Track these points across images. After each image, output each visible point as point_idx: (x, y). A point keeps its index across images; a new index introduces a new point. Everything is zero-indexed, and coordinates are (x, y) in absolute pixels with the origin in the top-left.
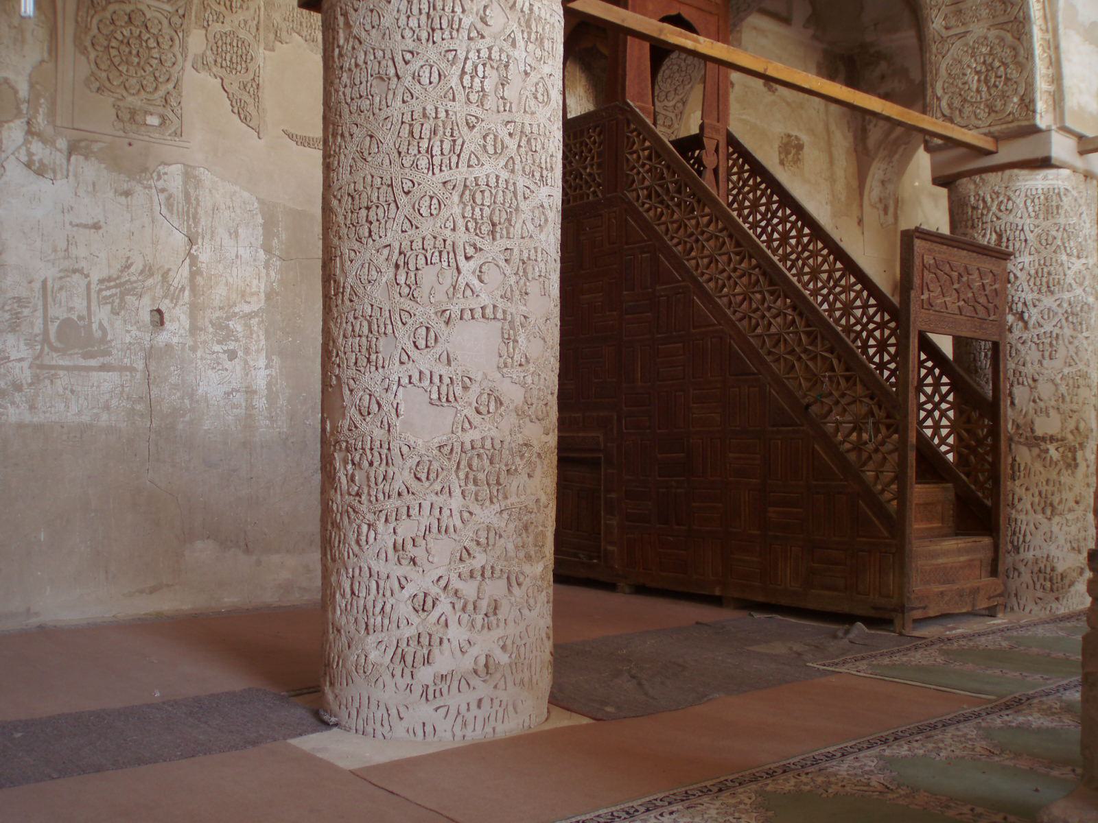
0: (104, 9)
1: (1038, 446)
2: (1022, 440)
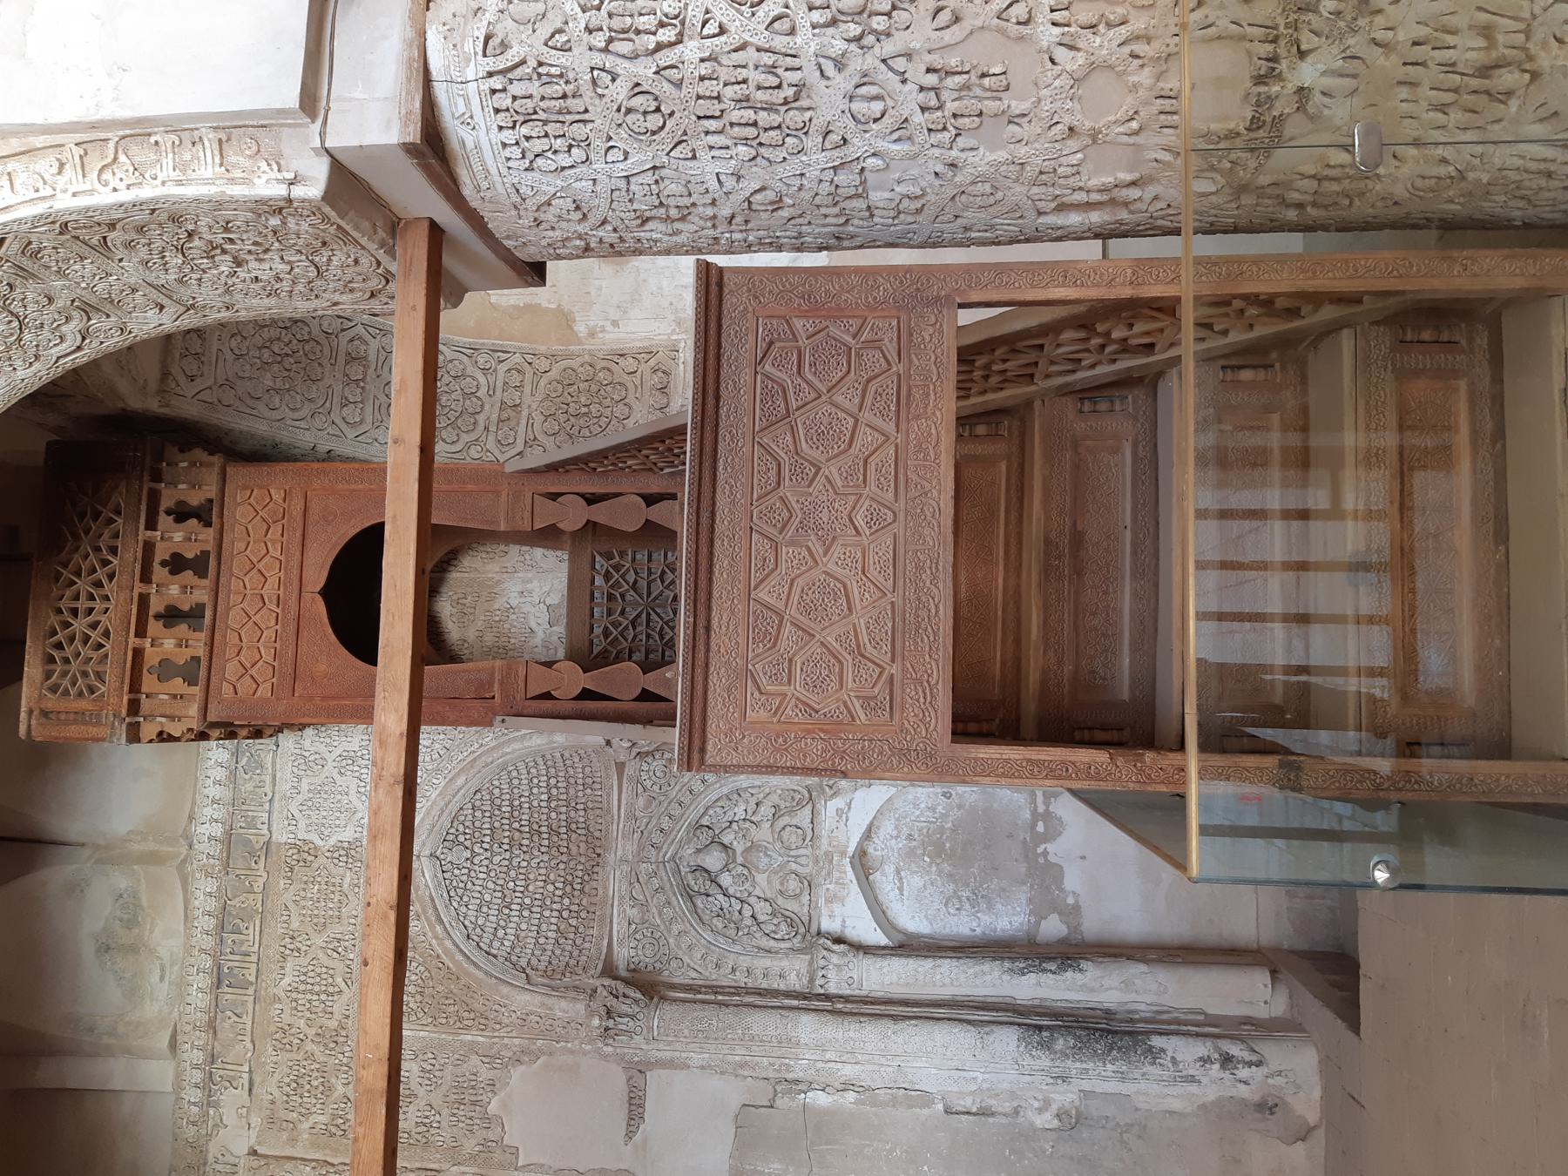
1: (1279, 121)
2: (1252, 164)
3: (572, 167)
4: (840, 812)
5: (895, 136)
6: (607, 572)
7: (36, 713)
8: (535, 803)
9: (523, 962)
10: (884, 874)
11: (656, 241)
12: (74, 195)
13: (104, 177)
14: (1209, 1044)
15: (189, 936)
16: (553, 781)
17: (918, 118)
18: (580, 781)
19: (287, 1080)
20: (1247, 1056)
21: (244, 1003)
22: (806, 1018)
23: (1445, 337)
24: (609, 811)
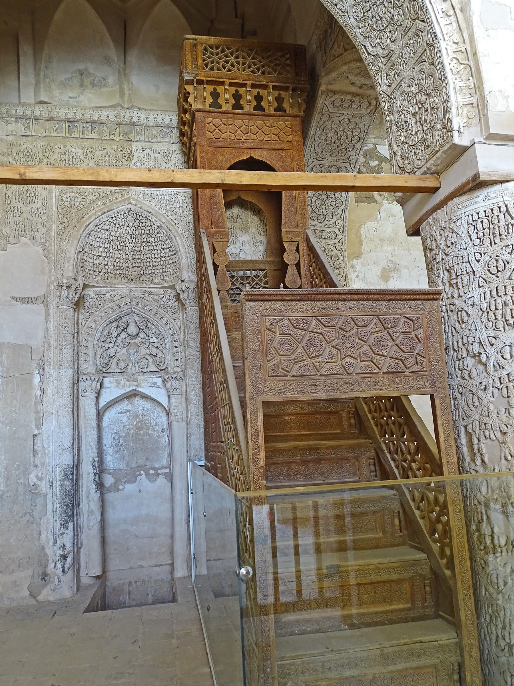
3: (471, 240)
4: (155, 383)
5: (496, 364)
6: (259, 276)
7: (195, 42)
8: (153, 252)
9: (86, 250)
10: (127, 405)
11: (438, 276)
12: (446, 48)
13: (454, 60)
14: (71, 549)
16: (163, 259)
17: (505, 373)
19: (30, 151)
20: (67, 566)
21: (62, 132)
22: (71, 371)
23: (428, 596)
24: (151, 283)
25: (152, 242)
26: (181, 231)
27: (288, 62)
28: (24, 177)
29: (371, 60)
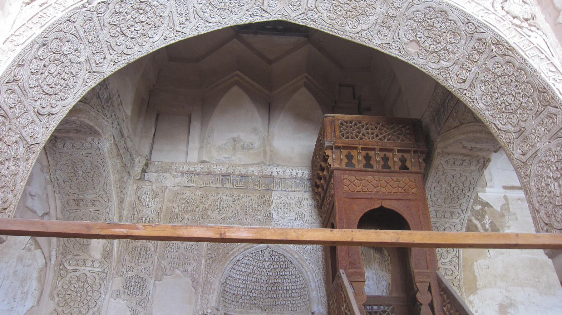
0: (66, 276)
8: (285, 284)
9: (228, 282)
15: (239, 166)
16: (294, 291)
18: (294, 302)
25: (285, 275)
26: (312, 266)
27: (408, 132)
28: (224, 237)
29: (502, 134)
